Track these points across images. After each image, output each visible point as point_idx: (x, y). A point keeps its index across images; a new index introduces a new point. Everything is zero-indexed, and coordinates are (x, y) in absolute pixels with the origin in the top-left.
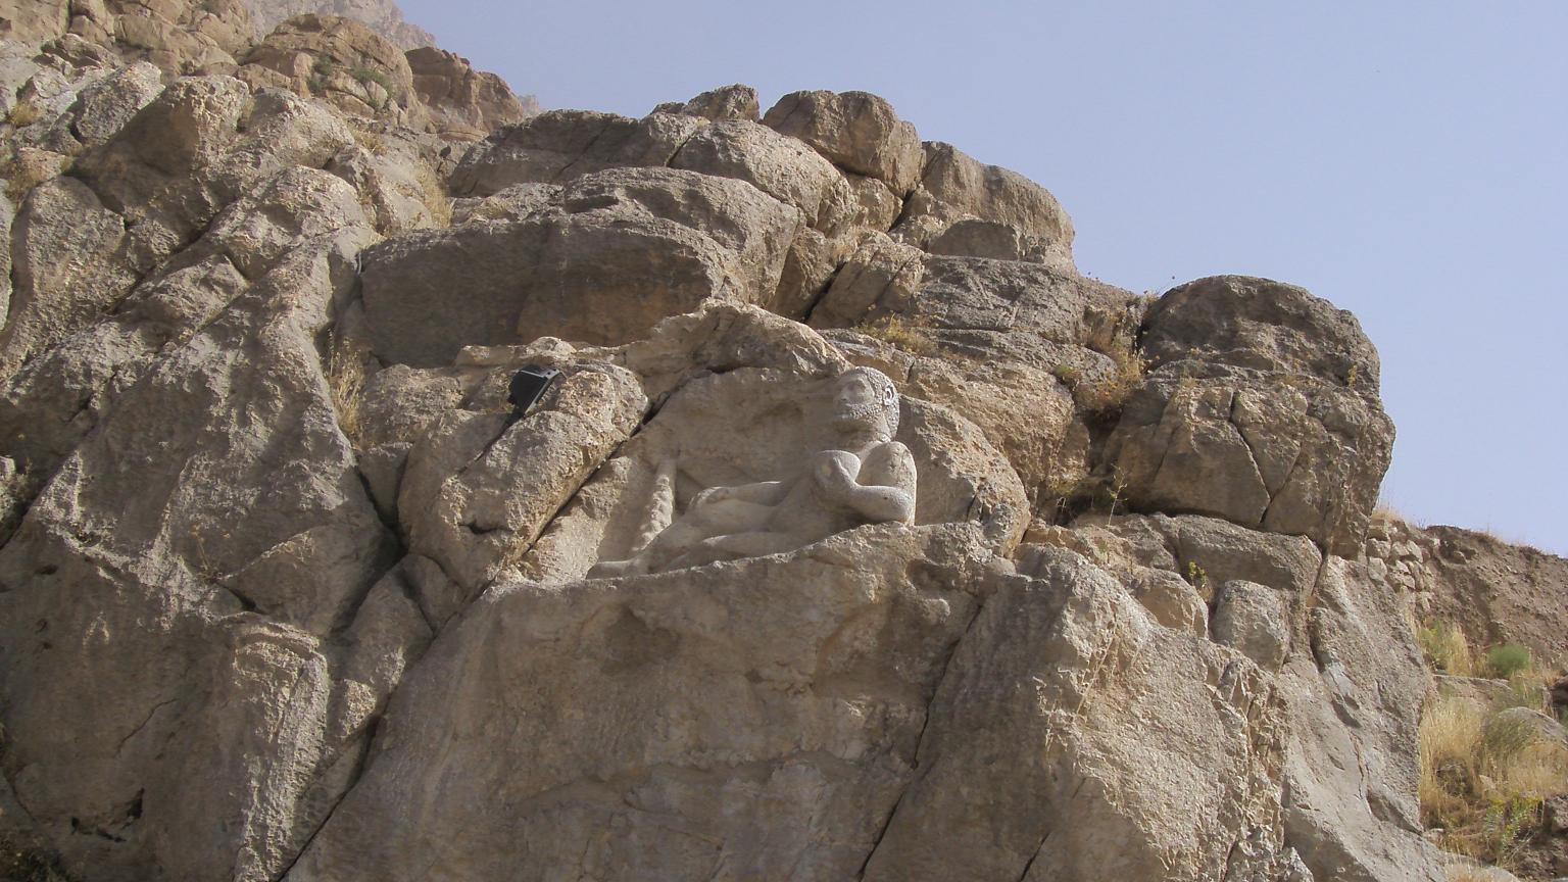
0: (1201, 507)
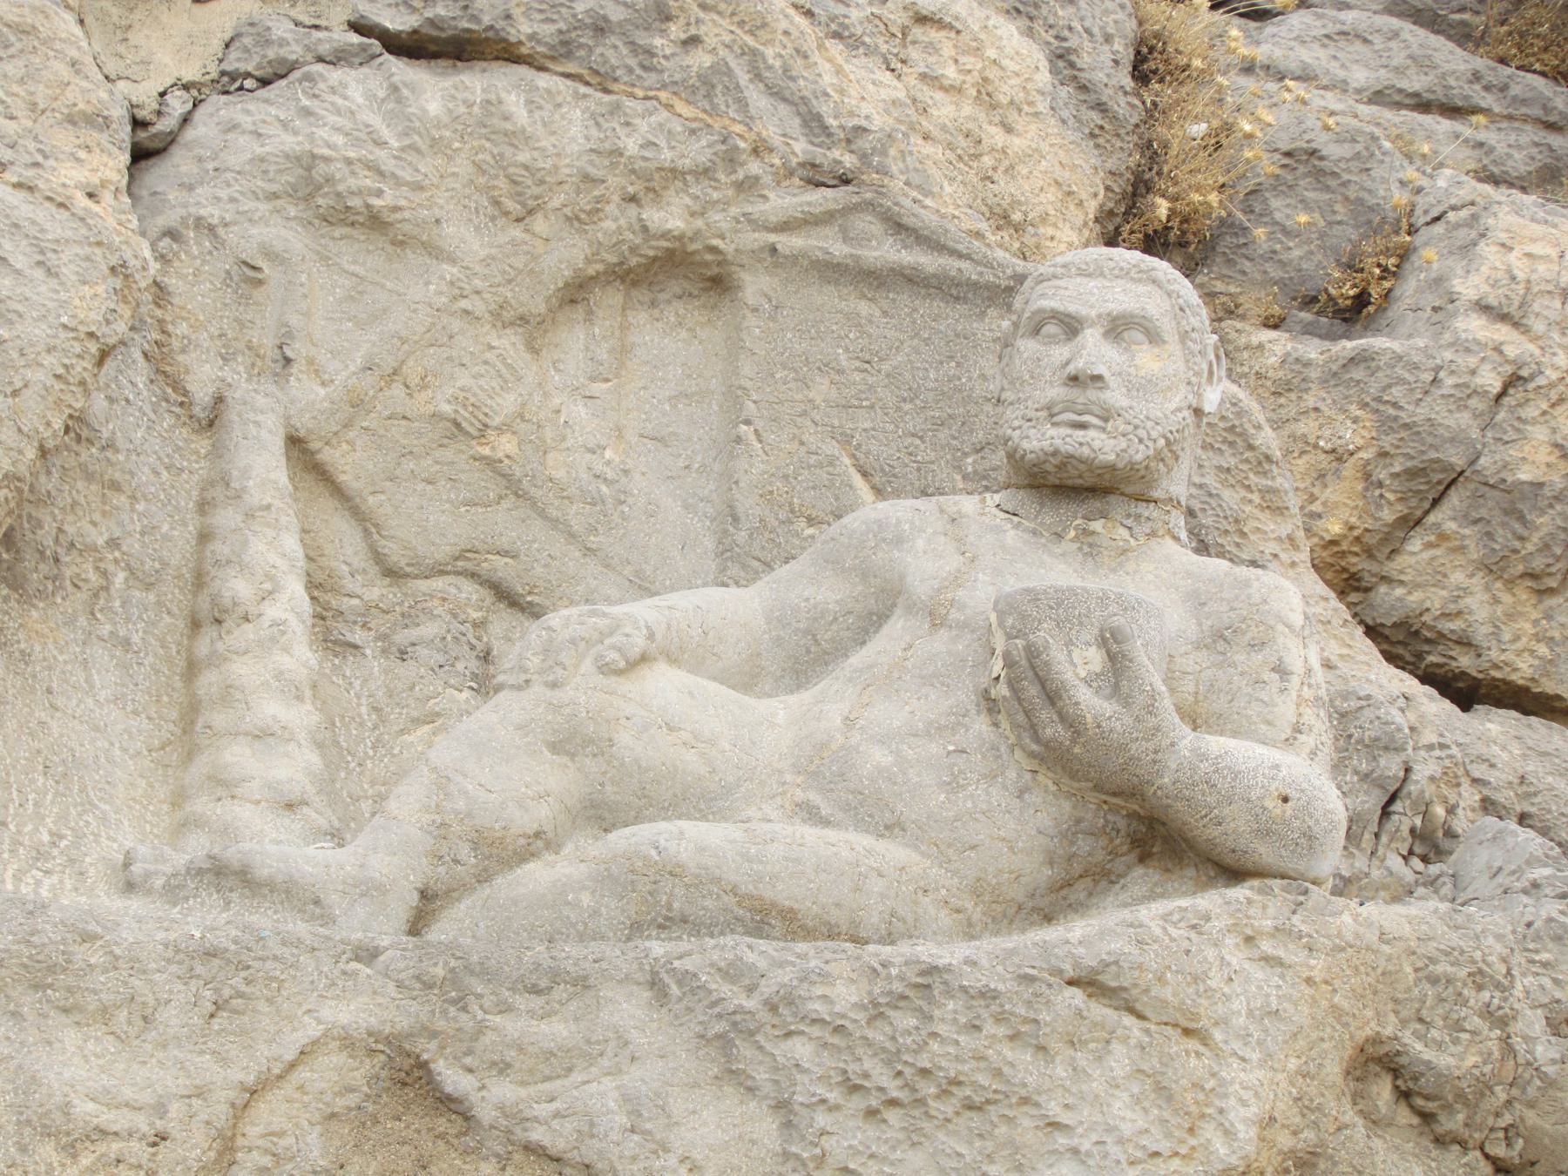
0: (1549, 687)
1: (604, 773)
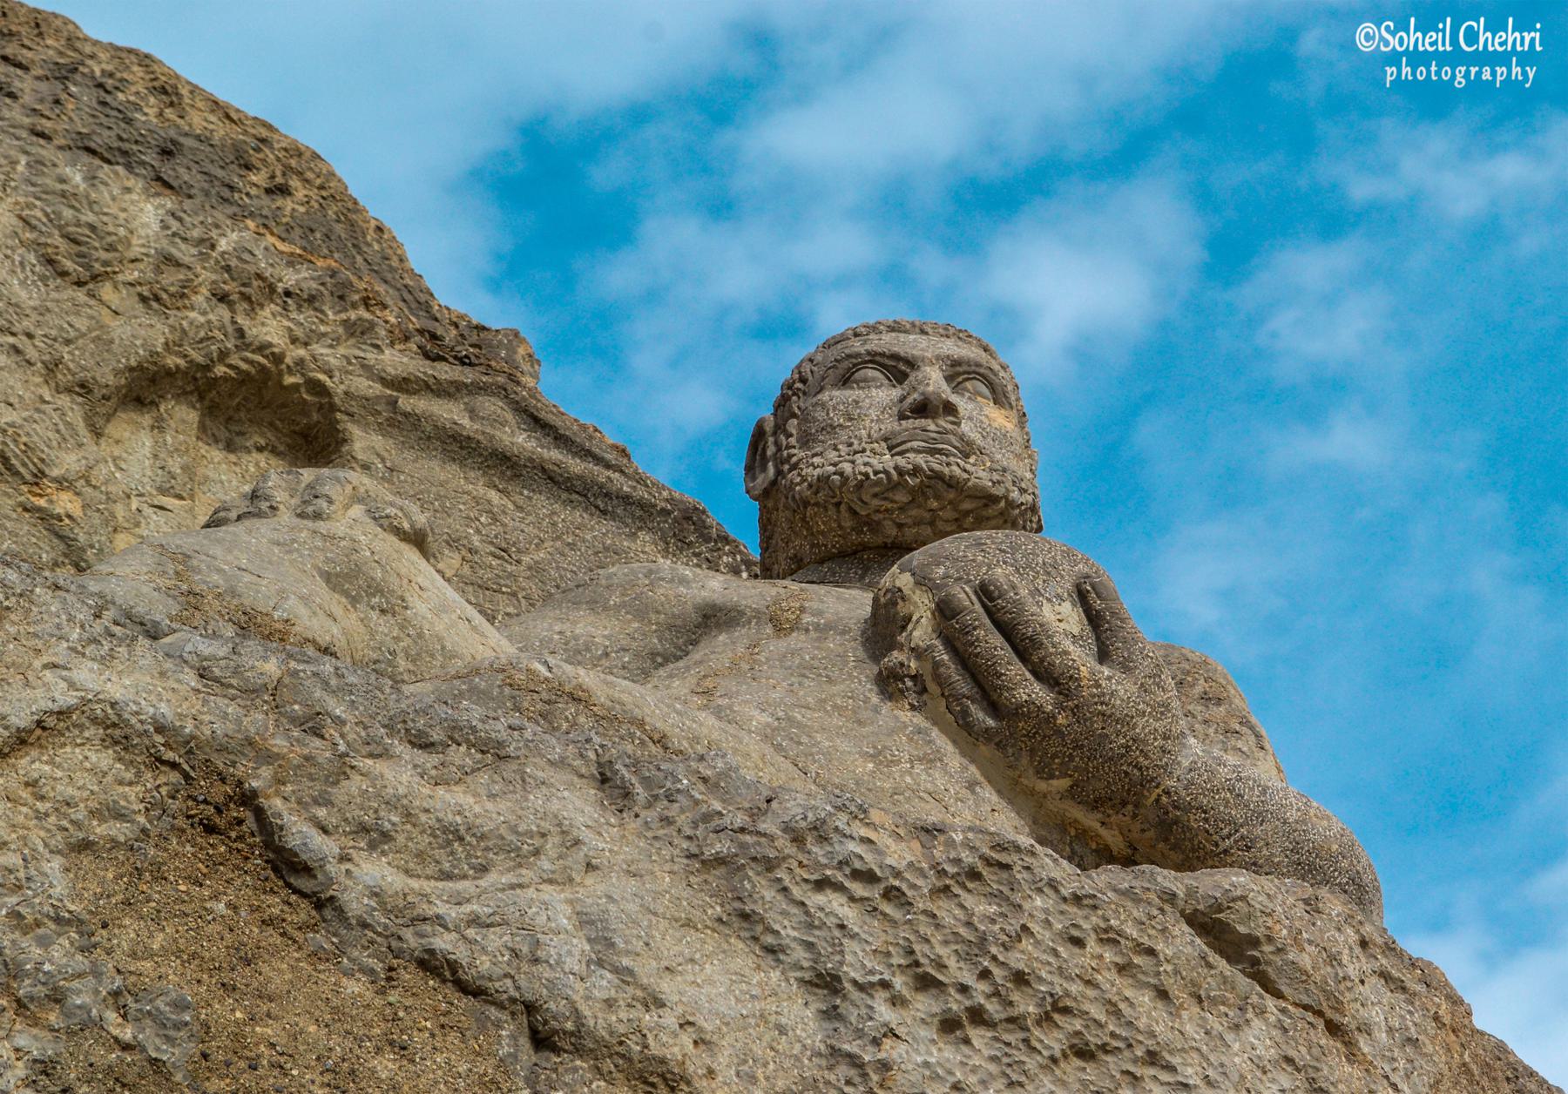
1: (397, 639)
